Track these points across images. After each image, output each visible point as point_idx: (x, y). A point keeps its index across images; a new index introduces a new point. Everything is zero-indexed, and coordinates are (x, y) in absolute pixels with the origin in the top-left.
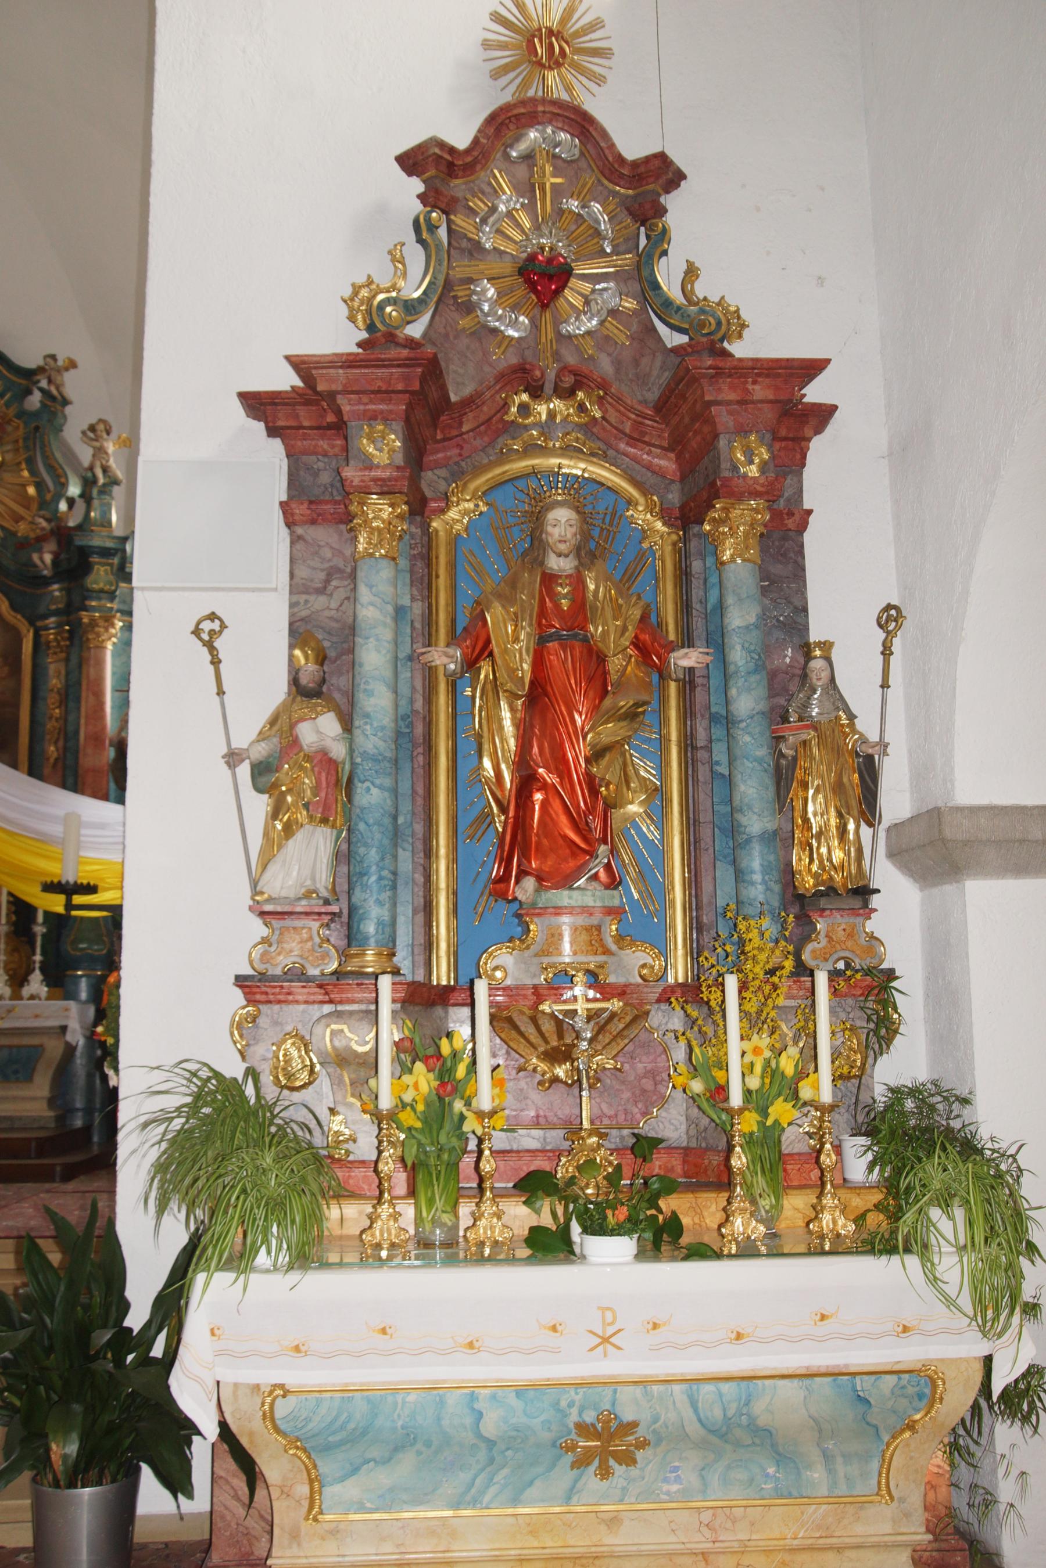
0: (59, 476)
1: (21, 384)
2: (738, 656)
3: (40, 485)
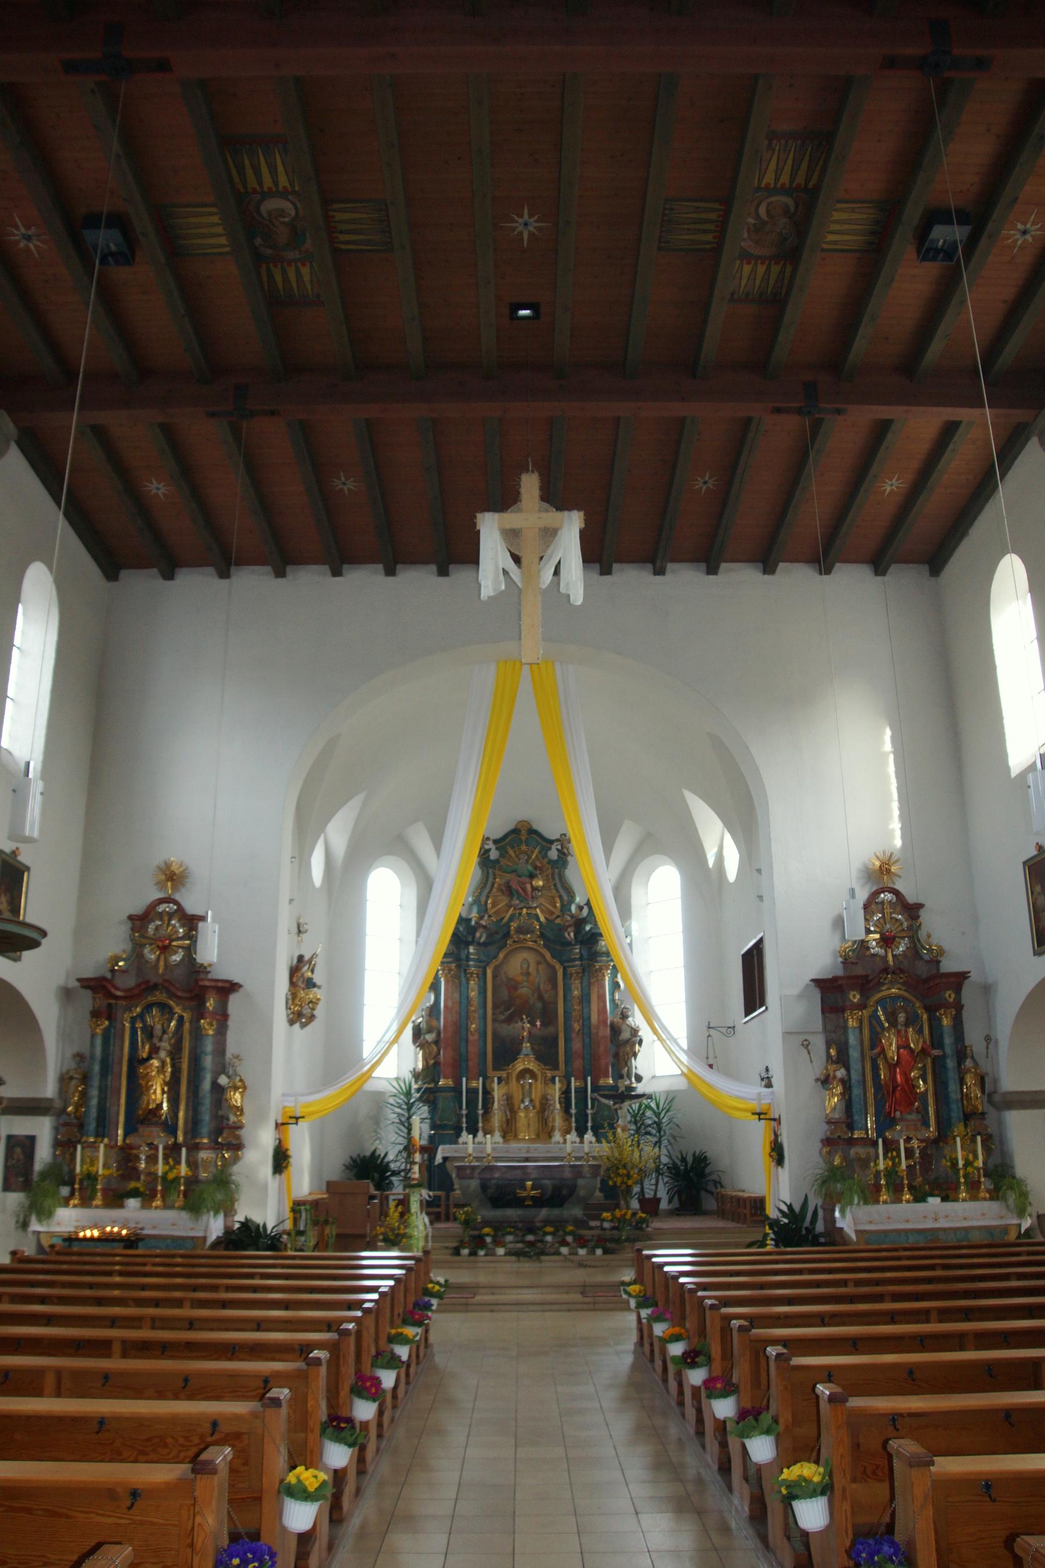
2: (948, 1050)
3: (560, 897)
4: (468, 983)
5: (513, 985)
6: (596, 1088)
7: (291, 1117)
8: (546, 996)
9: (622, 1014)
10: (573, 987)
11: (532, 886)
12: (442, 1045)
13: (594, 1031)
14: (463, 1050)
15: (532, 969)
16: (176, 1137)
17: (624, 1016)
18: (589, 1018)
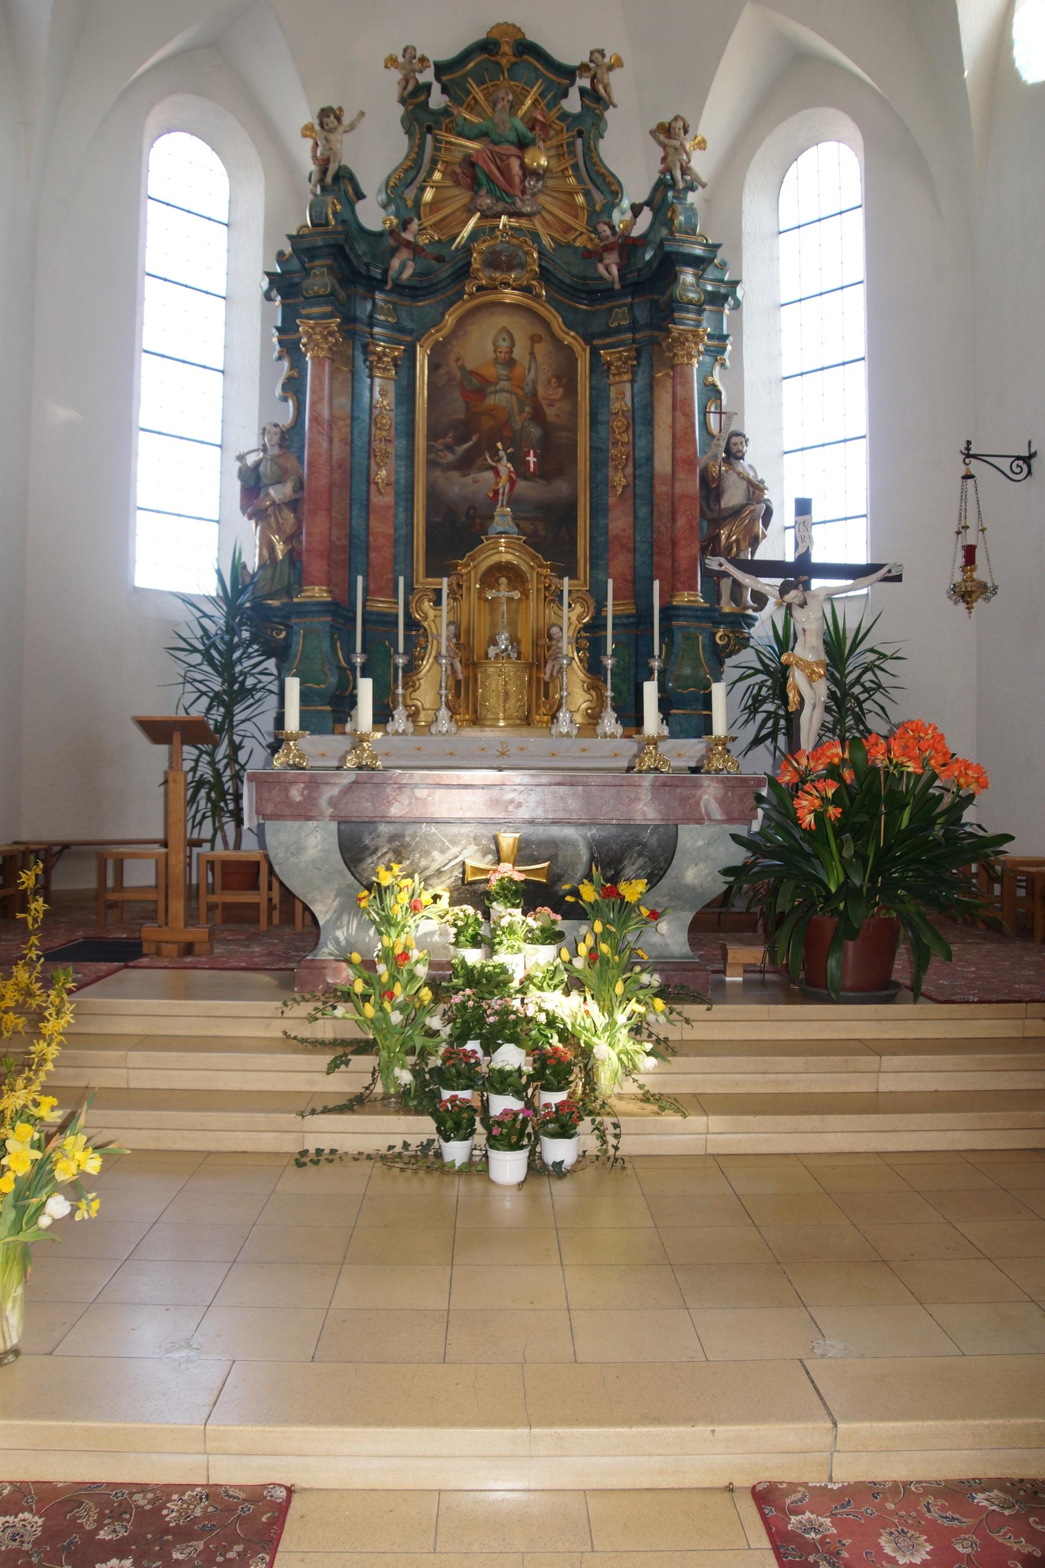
0: (609, 184)
1: (559, 84)
3: (587, 194)
4: (371, 377)
5: (477, 387)
6: (668, 612)
8: (550, 413)
9: (727, 451)
10: (613, 392)
11: (523, 166)
12: (306, 506)
13: (660, 489)
14: (358, 523)
15: (520, 352)
17: (733, 455)
18: (650, 459)
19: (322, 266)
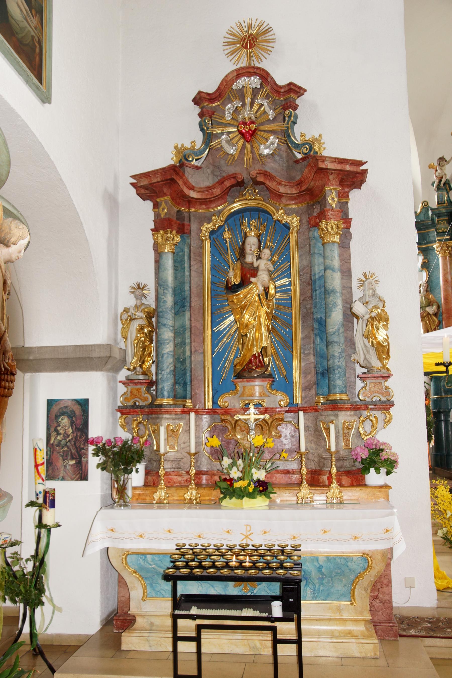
7: (437, 364)
16: (290, 393)
19: (444, 220)
